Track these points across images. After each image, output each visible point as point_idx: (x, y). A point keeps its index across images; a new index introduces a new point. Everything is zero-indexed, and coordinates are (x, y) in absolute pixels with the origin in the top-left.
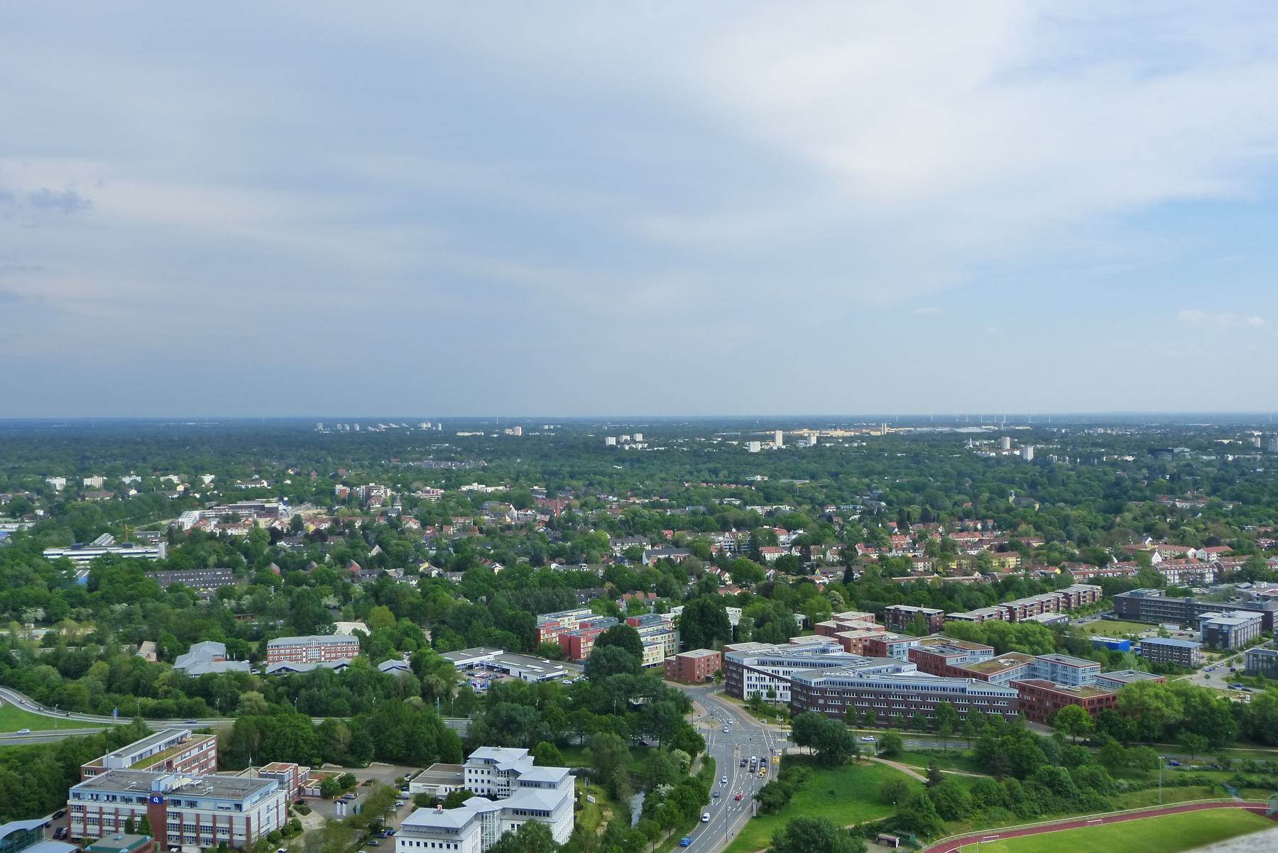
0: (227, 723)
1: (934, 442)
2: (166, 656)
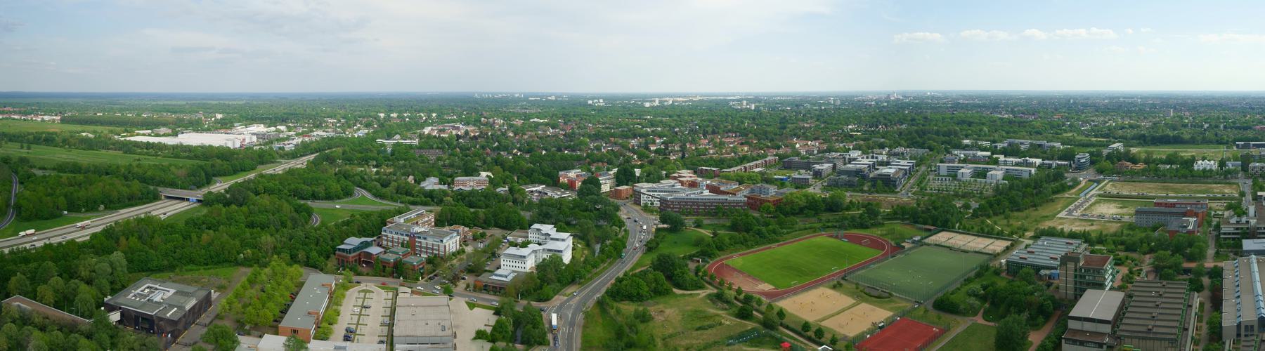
0: (439, 208)
1: (717, 103)
2: (418, 182)
